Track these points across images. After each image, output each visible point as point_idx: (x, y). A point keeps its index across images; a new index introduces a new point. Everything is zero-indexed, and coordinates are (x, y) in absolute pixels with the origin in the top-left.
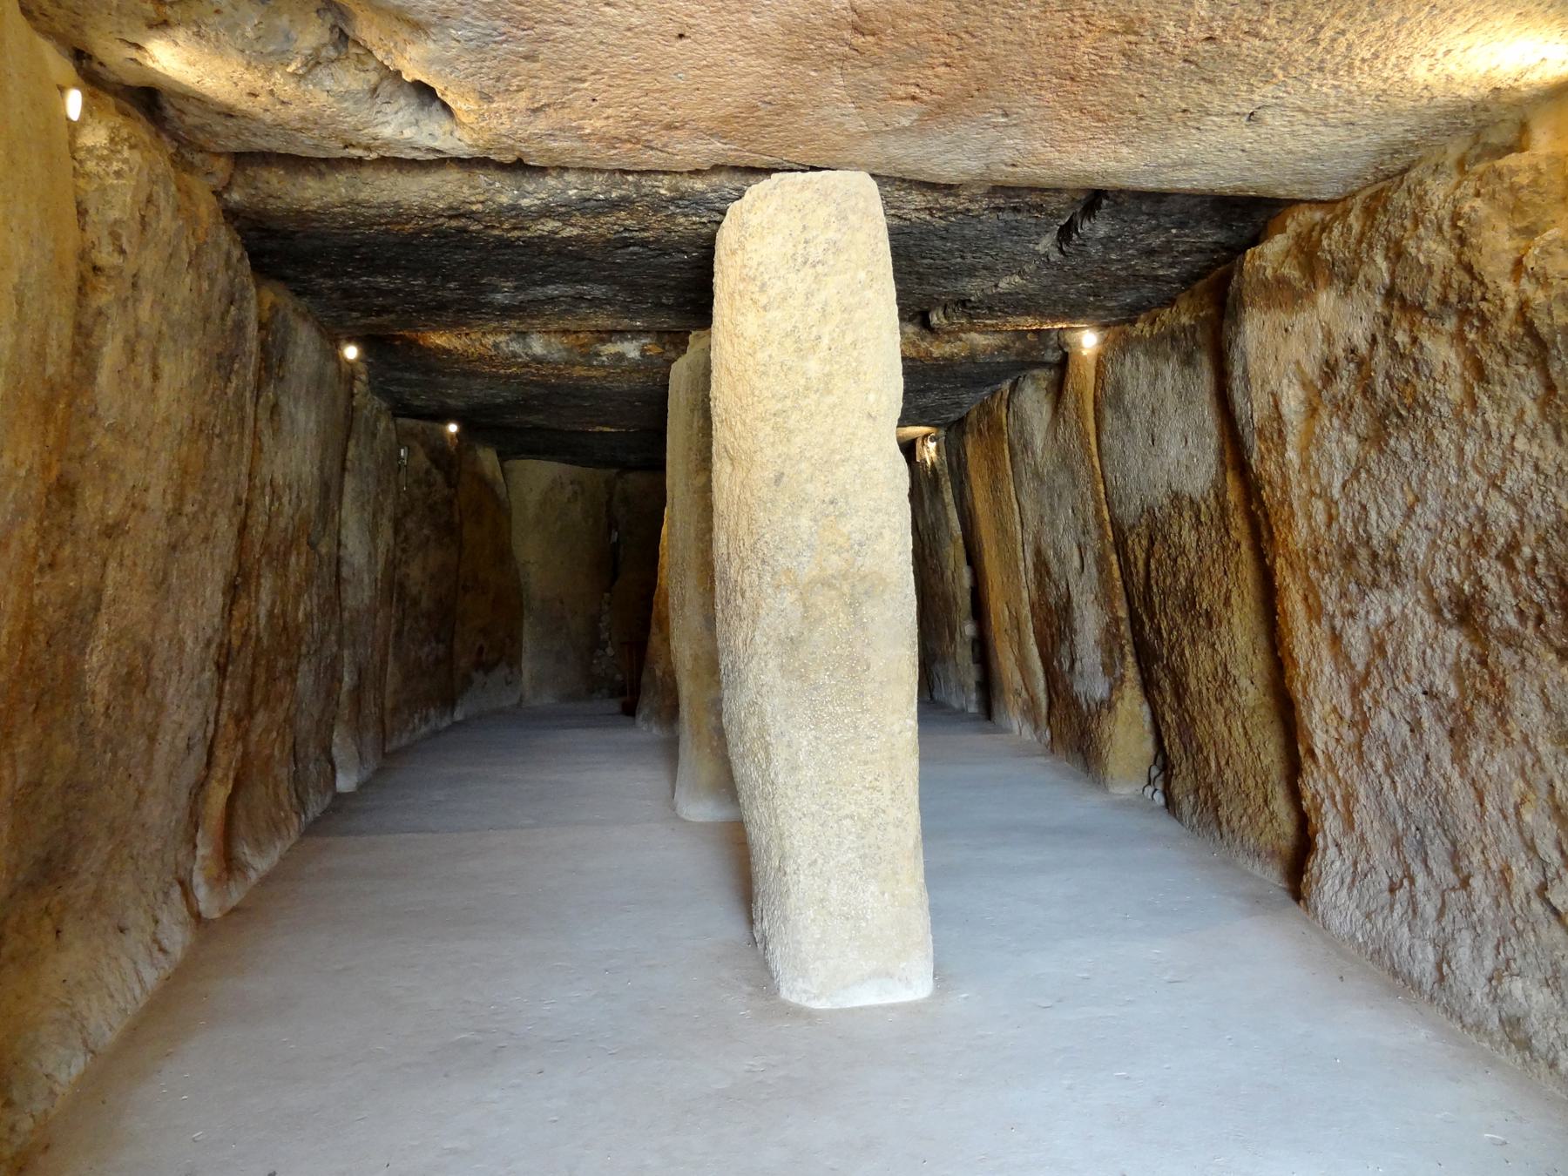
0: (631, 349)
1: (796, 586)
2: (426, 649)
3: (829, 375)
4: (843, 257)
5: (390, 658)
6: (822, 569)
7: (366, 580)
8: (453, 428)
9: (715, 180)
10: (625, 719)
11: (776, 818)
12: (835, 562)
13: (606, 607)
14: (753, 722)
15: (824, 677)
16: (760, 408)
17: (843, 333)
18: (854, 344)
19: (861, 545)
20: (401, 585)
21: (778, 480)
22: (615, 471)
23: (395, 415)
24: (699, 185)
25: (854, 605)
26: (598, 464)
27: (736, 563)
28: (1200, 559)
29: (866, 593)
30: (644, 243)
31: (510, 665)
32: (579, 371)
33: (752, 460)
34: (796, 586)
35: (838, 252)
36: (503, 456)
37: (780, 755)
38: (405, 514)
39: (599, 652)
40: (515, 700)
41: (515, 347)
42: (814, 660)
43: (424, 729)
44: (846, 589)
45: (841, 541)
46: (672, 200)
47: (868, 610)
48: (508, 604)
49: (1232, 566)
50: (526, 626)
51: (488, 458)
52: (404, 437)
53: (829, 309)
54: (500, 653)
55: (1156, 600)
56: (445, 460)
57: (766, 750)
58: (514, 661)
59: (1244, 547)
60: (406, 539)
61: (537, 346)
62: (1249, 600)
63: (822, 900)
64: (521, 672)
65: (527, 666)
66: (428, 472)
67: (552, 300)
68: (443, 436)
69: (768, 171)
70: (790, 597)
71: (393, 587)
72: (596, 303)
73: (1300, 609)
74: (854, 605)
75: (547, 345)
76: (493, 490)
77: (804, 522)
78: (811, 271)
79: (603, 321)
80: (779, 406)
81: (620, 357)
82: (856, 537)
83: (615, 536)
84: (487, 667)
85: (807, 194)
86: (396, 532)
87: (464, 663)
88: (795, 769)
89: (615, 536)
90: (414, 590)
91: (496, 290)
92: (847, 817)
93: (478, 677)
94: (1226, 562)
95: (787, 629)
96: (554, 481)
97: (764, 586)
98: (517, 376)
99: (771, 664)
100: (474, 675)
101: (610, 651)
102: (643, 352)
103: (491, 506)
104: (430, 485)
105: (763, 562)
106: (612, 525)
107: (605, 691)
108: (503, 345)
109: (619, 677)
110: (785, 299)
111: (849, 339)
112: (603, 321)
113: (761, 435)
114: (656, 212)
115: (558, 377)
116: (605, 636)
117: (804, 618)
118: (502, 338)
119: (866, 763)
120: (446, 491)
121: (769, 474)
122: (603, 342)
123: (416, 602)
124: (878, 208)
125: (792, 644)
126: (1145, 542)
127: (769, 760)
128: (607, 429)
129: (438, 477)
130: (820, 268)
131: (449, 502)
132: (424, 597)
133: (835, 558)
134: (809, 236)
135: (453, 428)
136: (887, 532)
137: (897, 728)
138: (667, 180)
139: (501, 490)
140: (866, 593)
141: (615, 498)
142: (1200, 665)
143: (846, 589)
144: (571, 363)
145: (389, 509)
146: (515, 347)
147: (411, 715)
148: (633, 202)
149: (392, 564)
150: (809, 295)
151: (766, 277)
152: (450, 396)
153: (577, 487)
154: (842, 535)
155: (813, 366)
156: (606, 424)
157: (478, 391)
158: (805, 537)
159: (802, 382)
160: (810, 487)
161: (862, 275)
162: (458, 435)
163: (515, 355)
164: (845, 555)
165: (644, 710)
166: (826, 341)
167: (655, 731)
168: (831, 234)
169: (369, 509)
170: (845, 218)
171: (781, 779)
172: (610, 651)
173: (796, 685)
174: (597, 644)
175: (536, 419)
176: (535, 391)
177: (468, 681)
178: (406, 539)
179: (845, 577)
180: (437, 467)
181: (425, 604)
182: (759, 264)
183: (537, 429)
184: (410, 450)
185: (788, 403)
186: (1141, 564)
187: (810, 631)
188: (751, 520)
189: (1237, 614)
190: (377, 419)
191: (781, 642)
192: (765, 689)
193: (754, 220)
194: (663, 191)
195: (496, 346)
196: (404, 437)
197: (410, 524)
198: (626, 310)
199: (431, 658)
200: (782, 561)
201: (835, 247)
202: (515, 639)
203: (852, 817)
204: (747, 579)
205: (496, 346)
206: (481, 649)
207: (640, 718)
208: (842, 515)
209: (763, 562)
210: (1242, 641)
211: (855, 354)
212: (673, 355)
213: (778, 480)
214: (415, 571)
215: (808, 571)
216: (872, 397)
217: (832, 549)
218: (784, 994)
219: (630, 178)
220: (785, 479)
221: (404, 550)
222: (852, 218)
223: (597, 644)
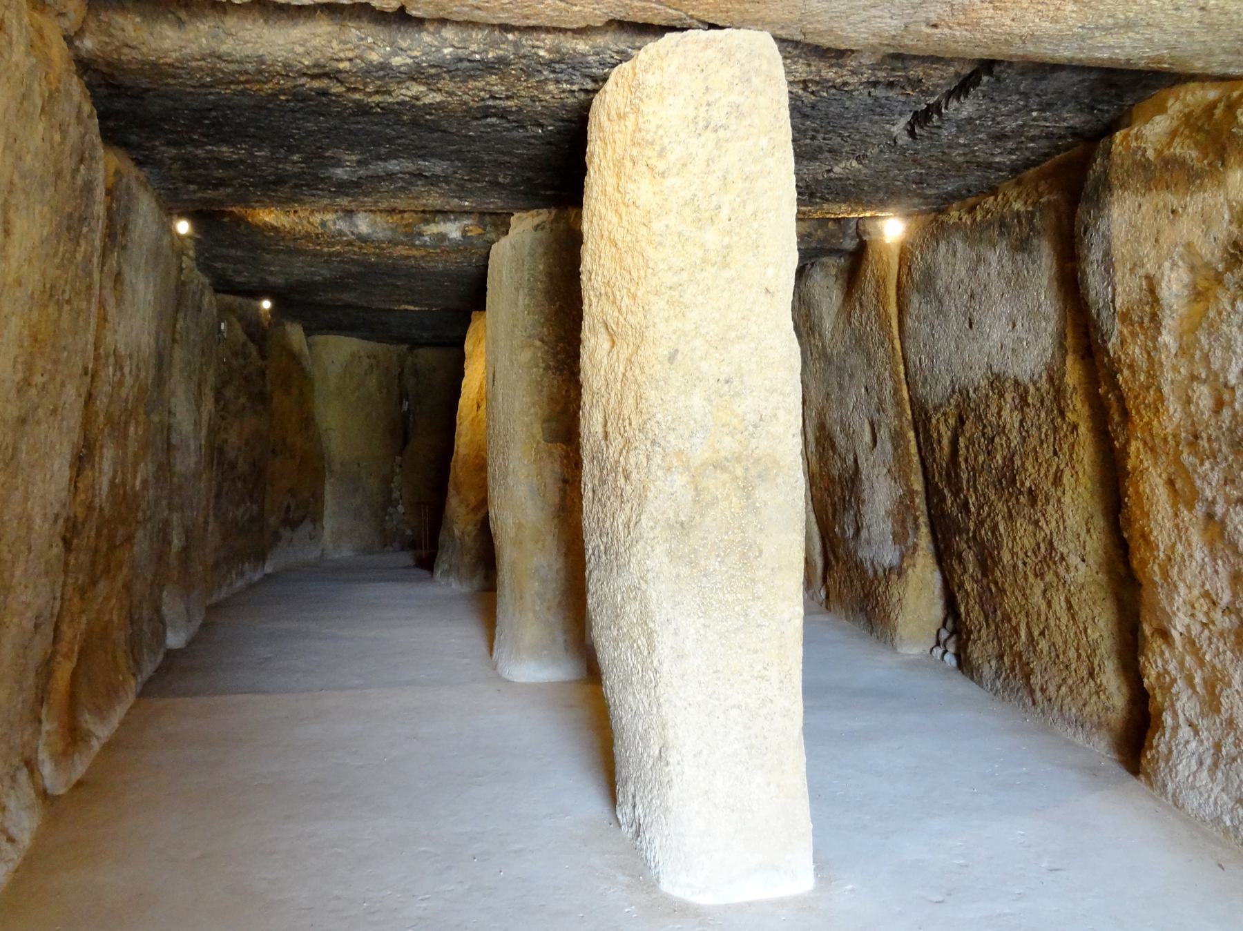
0: (452, 230)
1: (688, 469)
2: (241, 510)
3: (728, 247)
4: (746, 122)
5: (211, 519)
6: (716, 451)
7: (192, 447)
8: (266, 304)
9: (600, 40)
10: (425, 573)
11: (659, 706)
12: (728, 445)
13: (398, 470)
14: (632, 609)
15: (714, 564)
16: (654, 282)
17: (744, 202)
18: (755, 215)
19: (755, 426)
20: (221, 451)
21: (672, 358)
22: (405, 347)
23: (217, 291)
24: (582, 46)
25: (747, 490)
27: (617, 442)
28: (1024, 440)
29: (759, 476)
30: (503, 114)
31: (314, 521)
32: (401, 251)
33: (642, 335)
34: (688, 469)
35: (741, 116)
36: (308, 331)
37: (665, 645)
38: (225, 384)
39: (391, 510)
40: (317, 553)
41: (342, 225)
42: (704, 546)
43: (240, 584)
44: (739, 471)
45: (735, 422)
46: (549, 64)
47: (762, 494)
48: (313, 466)
49: (1065, 447)
50: (328, 488)
51: (295, 333)
52: (225, 312)
53: (730, 178)
54: (304, 513)
55: (964, 476)
56: (257, 332)
57: (649, 638)
58: (317, 519)
59: (1082, 429)
61: (363, 225)
62: (1084, 480)
63: (706, 792)
65: (329, 523)
66: (244, 345)
67: (390, 176)
68: (258, 309)
69: (658, 30)
70: (680, 480)
71: (216, 453)
72: (433, 181)
73: (1162, 493)
74: (747, 490)
75: (373, 224)
76: (300, 363)
77: (697, 401)
78: (713, 136)
79: (434, 200)
80: (676, 279)
81: (442, 237)
82: (752, 417)
83: (406, 406)
84: (293, 525)
85: (710, 53)
86: (217, 401)
87: (273, 521)
88: (680, 657)
89: (406, 406)
90: (231, 455)
91: (338, 163)
92: (734, 707)
93: (286, 533)
94: (1057, 443)
95: (677, 514)
97: (654, 468)
98: (339, 254)
99: (658, 549)
100: (281, 530)
101: (401, 509)
102: (464, 233)
103: (296, 376)
105: (654, 442)
107: (396, 545)
108: (330, 224)
109: (409, 532)
110: (684, 165)
111: (750, 209)
112: (434, 200)
113: (654, 309)
114: (529, 76)
115: (378, 255)
116: (396, 495)
117: (695, 501)
118: (329, 217)
119: (756, 652)
120: (260, 363)
121: (664, 352)
122: (427, 222)
123: (233, 466)
124: (780, 72)
125: (683, 528)
126: (952, 421)
127: (651, 647)
128: (412, 308)
129: (253, 349)
130: (721, 133)
131: (262, 373)
132: (241, 461)
133: (727, 439)
134: (711, 99)
135: (266, 304)
136: (781, 413)
137: (786, 616)
138: (549, 40)
139: (307, 363)
140: (759, 476)
142: (1017, 541)
143: (739, 471)
144: (393, 243)
145: (211, 378)
146: (342, 225)
147: (229, 571)
148: (508, 64)
149: (212, 431)
150: (709, 162)
151: (666, 141)
152: (271, 273)
153: (372, 361)
154: (736, 416)
155: (712, 237)
156: (408, 303)
157: (298, 269)
158: (699, 418)
159: (700, 253)
160: (704, 366)
161: (764, 142)
162: (271, 311)
163: (341, 233)
164: (739, 436)
165: (442, 563)
166: (725, 211)
167: (454, 586)
168: (734, 97)
169: (195, 378)
170: (749, 80)
171: (665, 668)
172: (401, 509)
173: (685, 571)
175: (348, 297)
176: (355, 269)
177: (276, 537)
178: (225, 408)
179: (738, 459)
180: (253, 341)
181: (242, 466)
182: (659, 127)
183: (348, 306)
184: (230, 325)
185: (685, 276)
186: (945, 442)
187: (702, 515)
188: (639, 399)
189: (1069, 494)
190: (202, 294)
191: (670, 527)
192: (650, 576)
193: (651, 80)
194: (542, 53)
195: (323, 224)
196: (225, 312)
198: (462, 191)
199: (246, 517)
200: (673, 442)
201: (737, 111)
202: (318, 497)
203: (739, 707)
204: (632, 460)
205: (323, 224)
206: (288, 507)
207: (438, 573)
208: (737, 394)
209: (654, 442)
210: (1074, 520)
211: (756, 225)
212: (493, 236)
213: (672, 358)
214: (233, 437)
215: (700, 453)
216: (771, 271)
217: (725, 430)
218: (665, 886)
219: (510, 36)
220: (679, 357)
221: (223, 418)
222: (755, 80)
223: (388, 502)
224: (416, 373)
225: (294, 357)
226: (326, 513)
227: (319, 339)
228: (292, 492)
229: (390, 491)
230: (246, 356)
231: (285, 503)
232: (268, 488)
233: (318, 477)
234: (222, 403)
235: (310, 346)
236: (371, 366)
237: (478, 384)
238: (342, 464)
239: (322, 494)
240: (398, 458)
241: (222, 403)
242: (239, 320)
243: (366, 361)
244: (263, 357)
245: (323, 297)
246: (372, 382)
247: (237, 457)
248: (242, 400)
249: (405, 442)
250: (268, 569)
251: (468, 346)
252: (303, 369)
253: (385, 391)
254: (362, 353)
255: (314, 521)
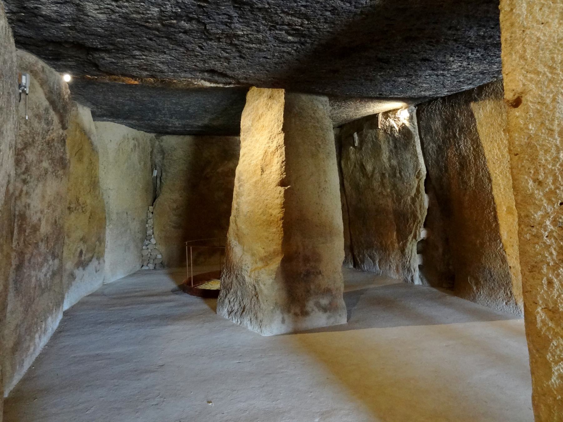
13: (151, 215)
22: (153, 135)
26: (149, 129)
36: (96, 116)
38: (26, 146)
39: (147, 242)
48: (98, 219)
50: (108, 231)
51: (84, 114)
60: (27, 170)
64: (104, 261)
66: (46, 110)
76: (89, 138)
83: (155, 173)
86: (18, 163)
89: (155, 173)
90: (35, 219)
96: (124, 137)
103: (86, 147)
104: (49, 123)
106: (153, 166)
109: (159, 256)
116: (150, 232)
120: (61, 131)
131: (63, 141)
132: (43, 223)
141: (155, 151)
153: (136, 143)
172: (153, 241)
174: (146, 237)
178: (27, 170)
180: (55, 109)
197: (31, 156)
199: (50, 273)
202: (101, 240)
207: (224, 312)
221: (25, 182)
223: (146, 237)
224: (162, 152)
225: (84, 132)
226: (106, 250)
227: (100, 124)
228: (83, 240)
229: (146, 230)
230: (49, 123)
231: (79, 250)
232: (67, 240)
233: (102, 227)
234: (24, 165)
235: (96, 128)
236: (135, 146)
237: (262, 152)
238: (117, 213)
239: (104, 237)
240: (151, 207)
241: (24, 165)
242: (42, 85)
243: (132, 142)
244: (64, 127)
245: (137, 57)
246: (135, 157)
247: (40, 220)
248: (45, 164)
249: (155, 199)
250: (66, 306)
251: (245, 121)
252: (91, 144)
253: (142, 163)
254: (129, 136)
255: (98, 259)
